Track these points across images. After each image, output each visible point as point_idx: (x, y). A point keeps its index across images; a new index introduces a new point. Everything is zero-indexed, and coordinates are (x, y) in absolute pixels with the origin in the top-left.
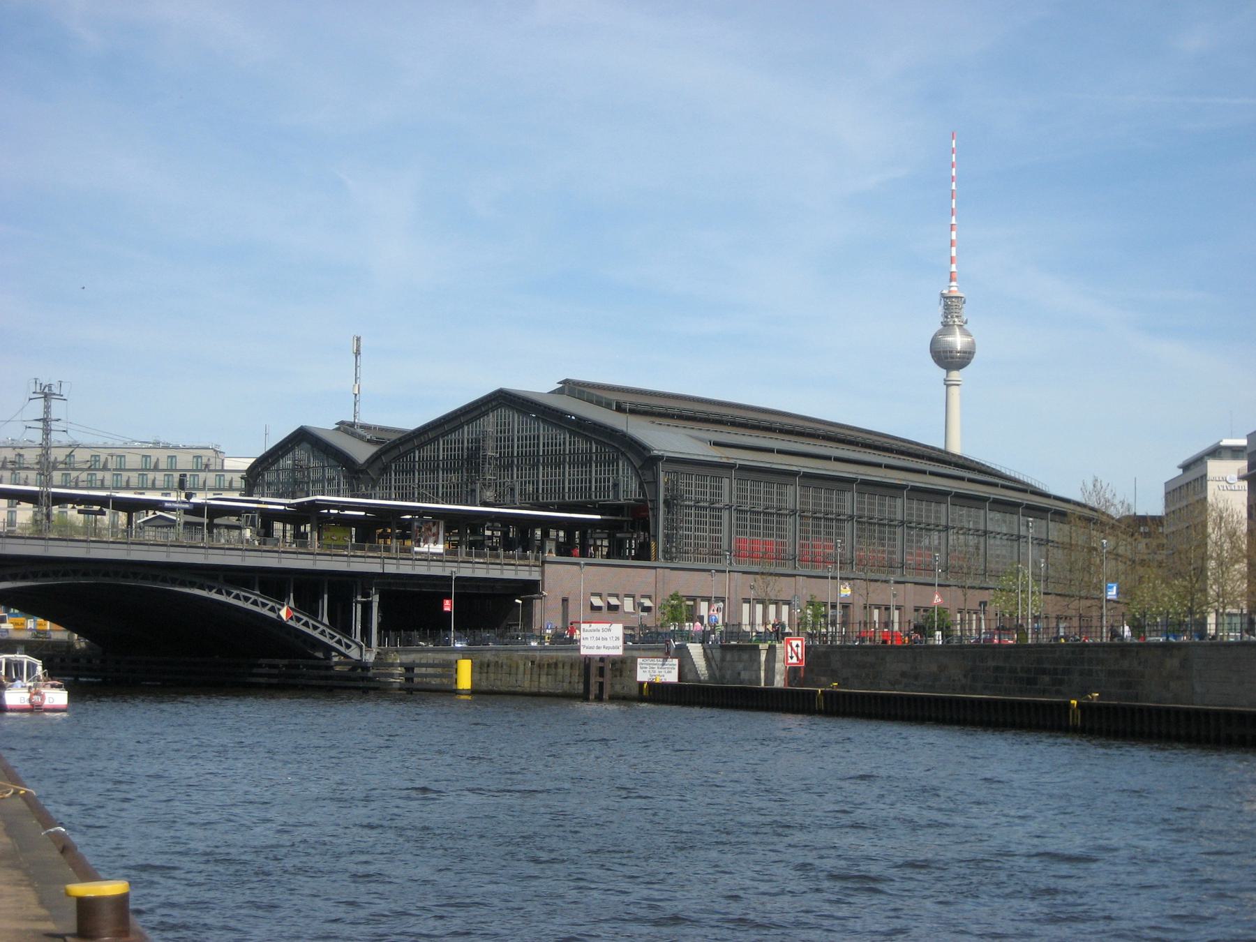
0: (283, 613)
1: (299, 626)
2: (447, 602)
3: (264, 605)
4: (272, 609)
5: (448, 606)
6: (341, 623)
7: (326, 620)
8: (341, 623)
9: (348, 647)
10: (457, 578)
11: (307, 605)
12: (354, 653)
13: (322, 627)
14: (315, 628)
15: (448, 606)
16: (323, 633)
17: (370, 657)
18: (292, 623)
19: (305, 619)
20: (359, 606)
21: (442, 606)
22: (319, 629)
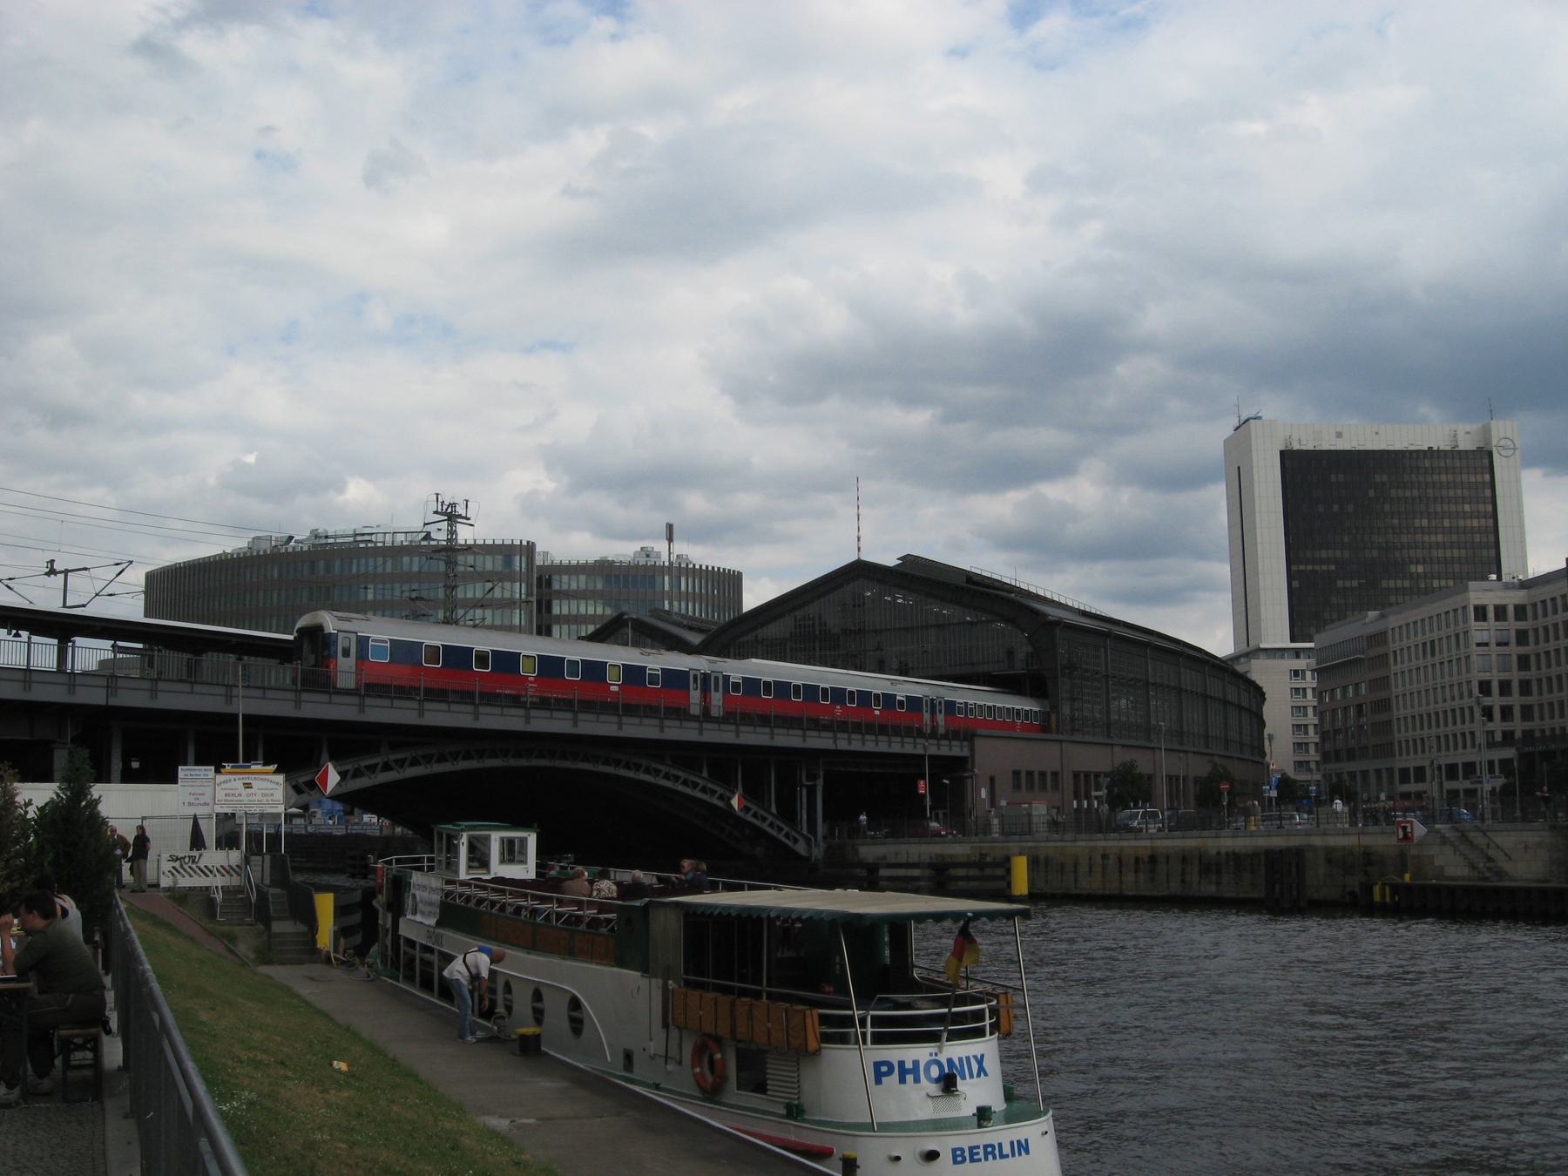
0: (735, 802)
1: (749, 818)
2: (921, 783)
3: (713, 792)
4: (721, 798)
5: (923, 787)
6: (788, 812)
7: (774, 810)
8: (788, 812)
9: (796, 841)
10: (931, 757)
11: (754, 792)
12: (801, 848)
13: (771, 819)
14: (764, 819)
15: (923, 787)
16: (771, 825)
17: (818, 853)
18: (742, 815)
19: (754, 808)
20: (804, 792)
21: (917, 788)
22: (768, 821)
